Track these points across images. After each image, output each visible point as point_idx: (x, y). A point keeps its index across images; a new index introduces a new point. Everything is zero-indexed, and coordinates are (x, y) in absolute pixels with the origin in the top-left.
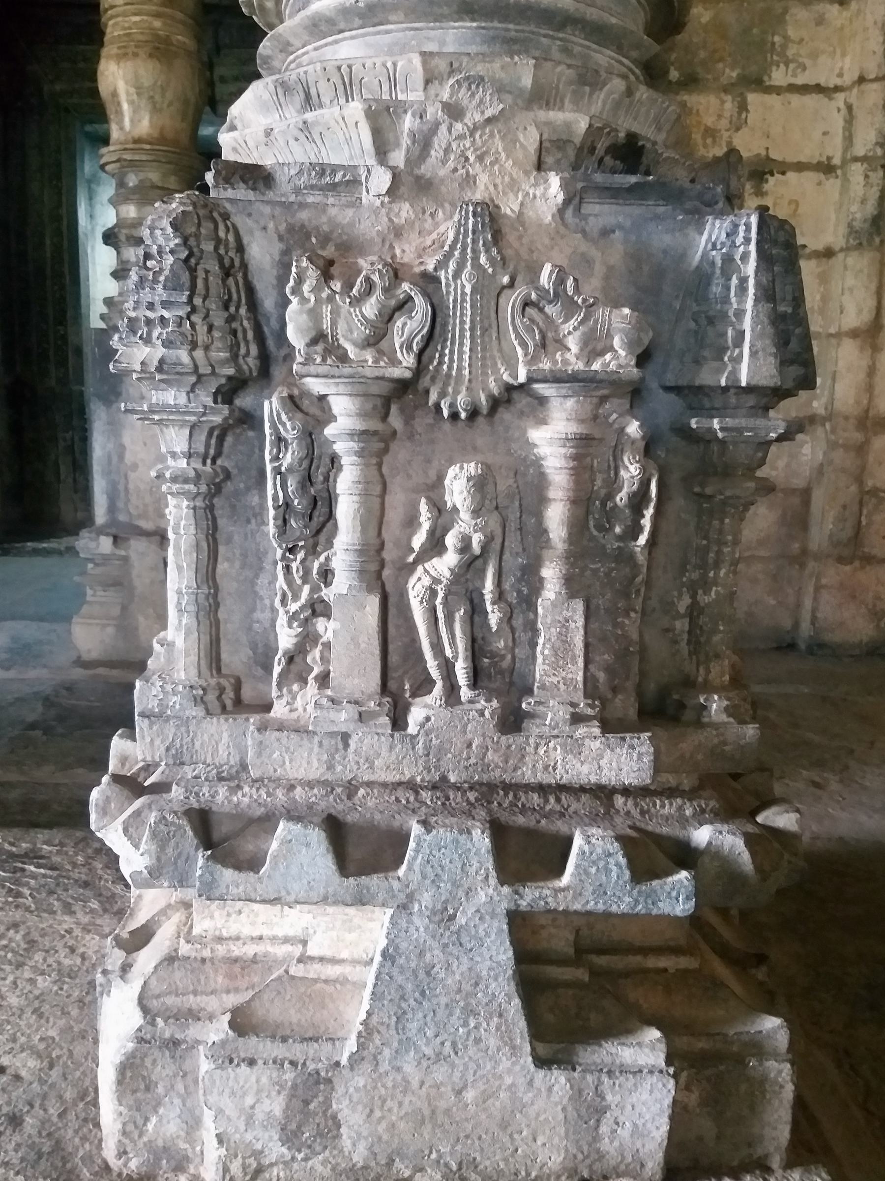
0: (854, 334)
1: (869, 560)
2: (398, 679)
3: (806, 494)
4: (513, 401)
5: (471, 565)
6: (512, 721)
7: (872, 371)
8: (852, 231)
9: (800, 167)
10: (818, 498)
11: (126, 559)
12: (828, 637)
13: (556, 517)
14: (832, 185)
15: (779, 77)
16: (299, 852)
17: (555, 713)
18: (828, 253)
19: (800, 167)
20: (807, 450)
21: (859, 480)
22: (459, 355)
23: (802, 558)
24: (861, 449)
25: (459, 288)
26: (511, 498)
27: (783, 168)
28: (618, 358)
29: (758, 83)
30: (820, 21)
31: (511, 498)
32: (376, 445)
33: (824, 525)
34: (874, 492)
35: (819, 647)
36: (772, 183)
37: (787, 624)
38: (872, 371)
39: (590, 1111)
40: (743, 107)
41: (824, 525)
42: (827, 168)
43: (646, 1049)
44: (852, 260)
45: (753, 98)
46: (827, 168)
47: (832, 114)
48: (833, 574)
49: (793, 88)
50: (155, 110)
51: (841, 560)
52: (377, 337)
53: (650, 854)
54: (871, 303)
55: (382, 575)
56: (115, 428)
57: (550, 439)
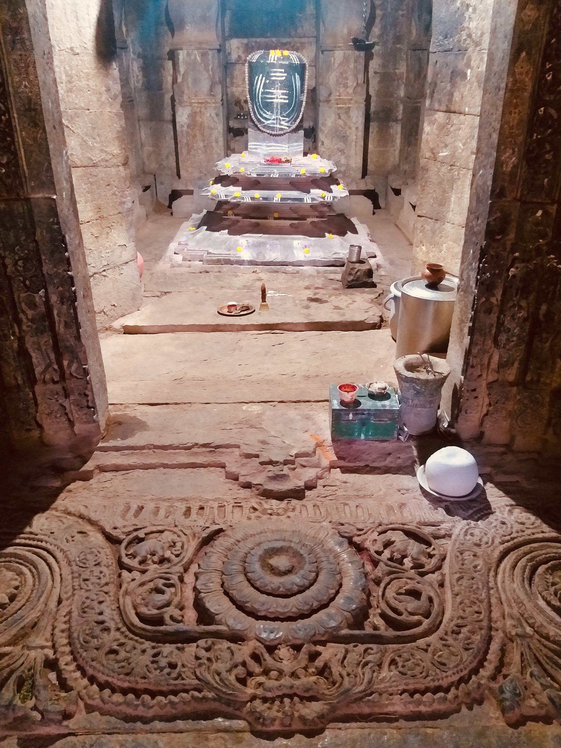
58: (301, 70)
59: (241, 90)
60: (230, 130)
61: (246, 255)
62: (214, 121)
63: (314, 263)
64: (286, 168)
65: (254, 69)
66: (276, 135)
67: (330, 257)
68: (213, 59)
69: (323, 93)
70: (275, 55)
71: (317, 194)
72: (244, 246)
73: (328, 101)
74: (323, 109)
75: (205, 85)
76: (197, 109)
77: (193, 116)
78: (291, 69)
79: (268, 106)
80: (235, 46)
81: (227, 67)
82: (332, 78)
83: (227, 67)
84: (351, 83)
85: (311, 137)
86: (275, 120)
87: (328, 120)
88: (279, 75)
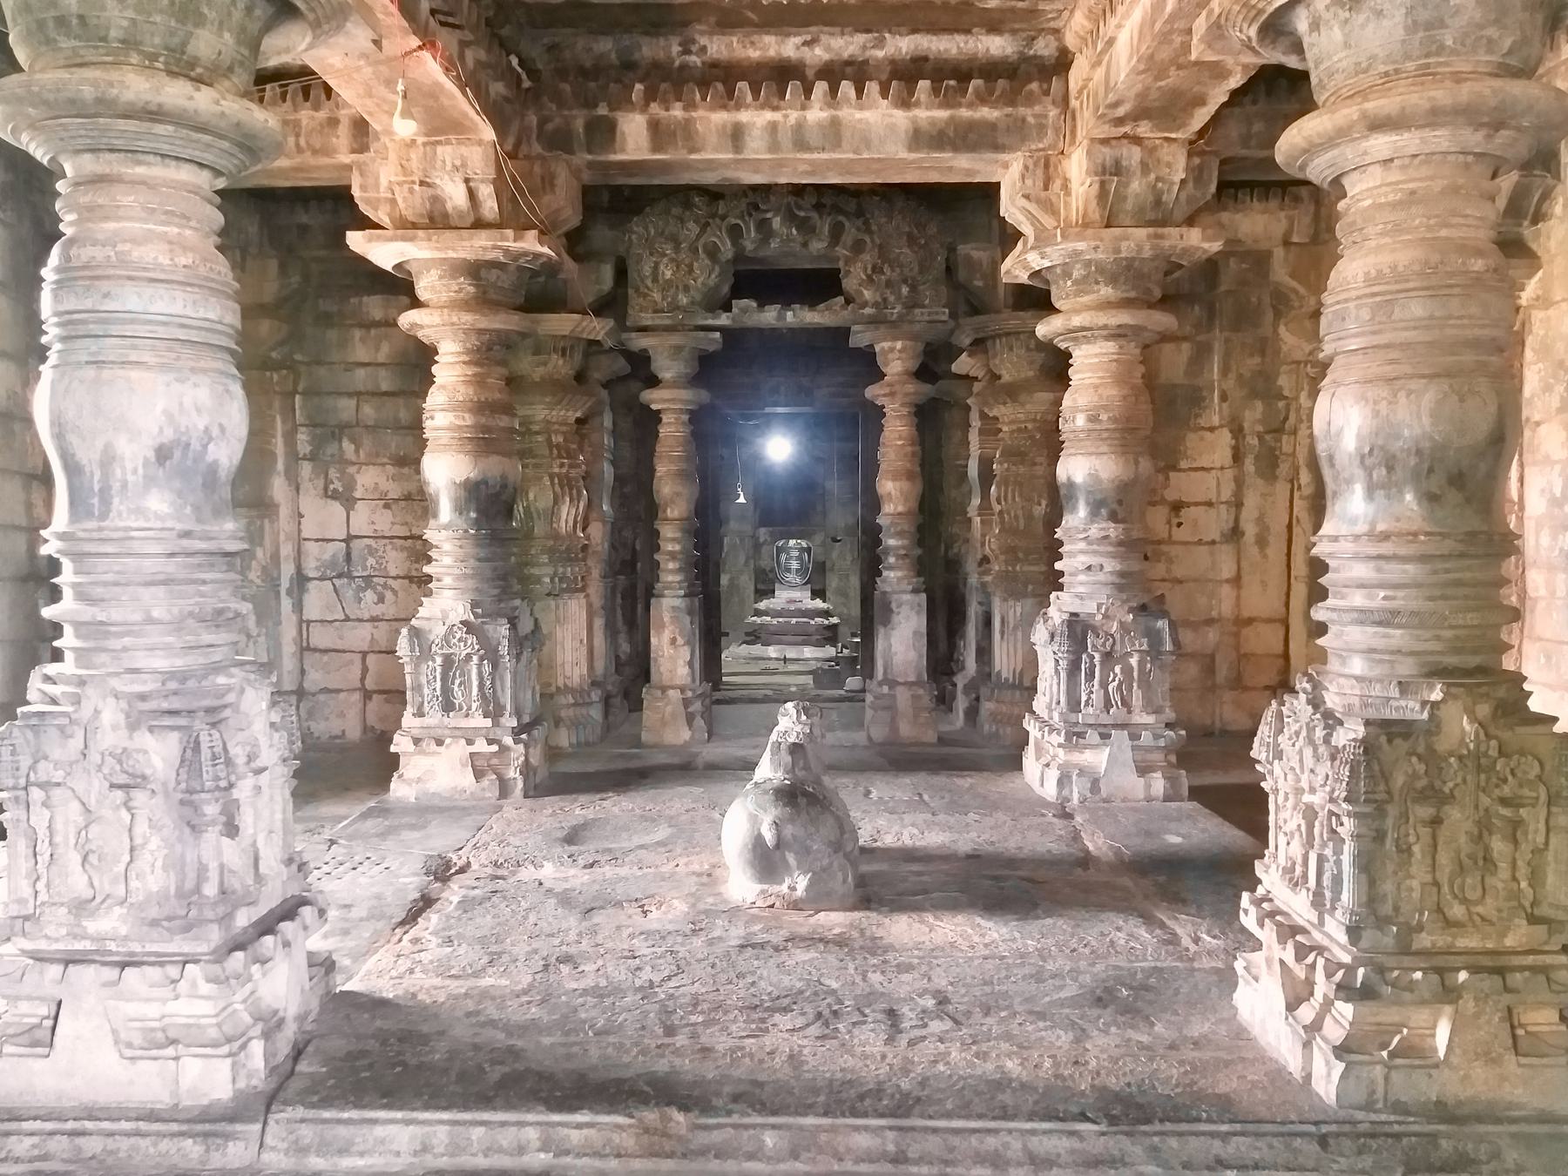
0: (1227, 581)
1: (1246, 689)
2: (1108, 704)
3: (1212, 657)
4: (1130, 654)
5: (1120, 684)
6: (1129, 712)
7: (1238, 598)
8: (1223, 535)
9: (1197, 504)
10: (1218, 658)
11: (894, 696)
12: (1229, 728)
13: (1135, 674)
14: (1213, 512)
15: (1183, 464)
16: (1092, 736)
17: (1137, 711)
18: (1213, 542)
19: (1197, 504)
20: (1211, 635)
21: (1237, 647)
22: (1118, 647)
23: (1213, 688)
24: (1237, 635)
25: (1118, 637)
26: (1127, 671)
27: (1188, 505)
28: (1145, 647)
29: (1175, 468)
30: (1202, 439)
31: (1127, 671)
32: (1102, 663)
33: (1223, 672)
34: (1245, 655)
35: (1224, 732)
36: (1183, 512)
37: (1208, 722)
38: (1238, 598)
39: (1148, 786)
40: (1167, 478)
41: (1223, 672)
42: (1210, 504)
43: (1158, 775)
44: (1225, 547)
45: (1171, 474)
46: (1210, 504)
47: (1210, 479)
48: (1228, 696)
49: (1191, 469)
50: (906, 500)
51: (1232, 689)
52: (1104, 645)
53: (1156, 737)
54: (1235, 567)
55: (1104, 685)
56: (888, 637)
57: (1134, 661)
58: (809, 550)
59: (765, 563)
60: (757, 591)
61: (774, 655)
62: (747, 583)
63: (817, 659)
64: (799, 605)
65: (780, 551)
66: (793, 587)
67: (827, 656)
68: (748, 543)
69: (828, 565)
70: (792, 542)
71: (819, 620)
72: (772, 651)
73: (832, 570)
74: (828, 574)
75: (742, 559)
76: (735, 575)
77: (731, 580)
78: (802, 550)
79: (789, 570)
80: (763, 533)
81: (757, 547)
82: (834, 555)
83: (757, 547)
84: (849, 558)
85: (818, 593)
86: (792, 577)
87: (833, 582)
88: (795, 553)
